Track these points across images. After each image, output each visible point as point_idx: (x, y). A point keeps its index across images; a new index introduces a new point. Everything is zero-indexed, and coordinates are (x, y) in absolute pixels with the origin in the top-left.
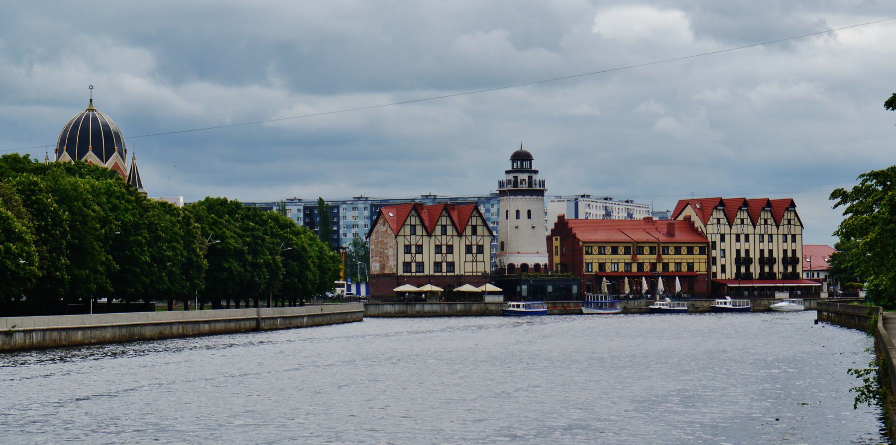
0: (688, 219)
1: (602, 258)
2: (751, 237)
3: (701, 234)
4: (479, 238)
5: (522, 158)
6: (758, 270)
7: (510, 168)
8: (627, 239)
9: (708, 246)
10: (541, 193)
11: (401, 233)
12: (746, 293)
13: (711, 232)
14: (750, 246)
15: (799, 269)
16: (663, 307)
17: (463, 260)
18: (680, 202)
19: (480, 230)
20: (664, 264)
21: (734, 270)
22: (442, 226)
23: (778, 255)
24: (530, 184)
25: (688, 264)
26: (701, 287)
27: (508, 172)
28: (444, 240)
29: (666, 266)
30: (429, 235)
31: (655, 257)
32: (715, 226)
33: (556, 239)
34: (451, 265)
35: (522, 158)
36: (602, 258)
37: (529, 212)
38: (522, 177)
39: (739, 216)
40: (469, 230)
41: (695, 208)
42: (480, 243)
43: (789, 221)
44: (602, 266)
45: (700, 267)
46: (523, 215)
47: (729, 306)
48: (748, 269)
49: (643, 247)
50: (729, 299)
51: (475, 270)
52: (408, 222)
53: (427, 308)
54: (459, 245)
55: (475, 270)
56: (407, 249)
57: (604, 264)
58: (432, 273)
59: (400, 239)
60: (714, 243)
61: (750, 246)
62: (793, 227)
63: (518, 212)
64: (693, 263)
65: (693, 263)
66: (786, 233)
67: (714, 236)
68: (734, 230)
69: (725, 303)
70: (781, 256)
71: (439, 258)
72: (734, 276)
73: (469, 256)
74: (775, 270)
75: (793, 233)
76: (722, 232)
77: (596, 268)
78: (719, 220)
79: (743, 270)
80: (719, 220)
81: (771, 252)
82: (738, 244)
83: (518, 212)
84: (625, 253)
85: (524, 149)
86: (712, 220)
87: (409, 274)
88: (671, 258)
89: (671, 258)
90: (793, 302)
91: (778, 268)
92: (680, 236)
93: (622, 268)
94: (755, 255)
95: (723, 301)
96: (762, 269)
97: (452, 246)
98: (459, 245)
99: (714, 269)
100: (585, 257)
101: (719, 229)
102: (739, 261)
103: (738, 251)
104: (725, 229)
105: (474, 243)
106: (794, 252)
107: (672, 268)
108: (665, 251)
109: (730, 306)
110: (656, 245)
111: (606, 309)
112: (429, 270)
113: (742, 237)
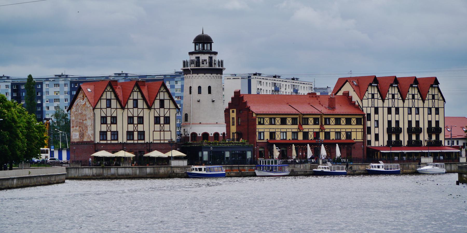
0: (346, 94)
1: (272, 128)
2: (401, 110)
3: (358, 107)
4: (166, 110)
5: (203, 41)
6: (407, 139)
7: (193, 50)
8: (294, 111)
9: (364, 118)
10: (219, 71)
11: (98, 106)
12: (396, 158)
13: (367, 105)
14: (400, 117)
15: (442, 138)
16: (325, 170)
17: (152, 129)
18: (340, 80)
19: (167, 103)
20: (325, 133)
22: (134, 100)
23: (424, 125)
24: (211, 64)
25: (347, 133)
26: (358, 153)
27: (191, 53)
28: (136, 112)
29: (327, 135)
30: (123, 108)
31: (318, 127)
32: (370, 100)
33: (233, 112)
34: (142, 134)
35: (203, 41)
36: (272, 128)
37: (210, 88)
38: (204, 57)
39: (390, 92)
40: (157, 104)
41: (352, 85)
42: (167, 115)
43: (433, 96)
44: (272, 135)
45: (357, 136)
46: (205, 90)
47: (381, 169)
48: (398, 137)
49: (308, 118)
50: (382, 164)
51: (162, 138)
52: (104, 97)
53: (121, 171)
54: (149, 116)
55: (162, 138)
56: (104, 120)
57: (275, 133)
58: (125, 141)
59: (97, 112)
60: (369, 115)
61: (400, 117)
62: (436, 101)
63: (200, 88)
64: (351, 132)
65: (351, 132)
66: (431, 106)
67: (369, 109)
68: (386, 104)
69: (379, 167)
70: (426, 126)
71: (131, 128)
72: (386, 144)
73: (157, 126)
74: (421, 138)
75: (436, 106)
76: (376, 106)
77: (267, 137)
78: (373, 95)
79: (394, 138)
80: (373, 95)
81: (417, 122)
82: (390, 116)
83: (200, 88)
84: (292, 124)
85: (204, 33)
86: (368, 95)
87: (105, 142)
88: (332, 128)
89: (332, 128)
90: (437, 166)
91: (424, 137)
92: (340, 109)
93: (289, 137)
94: (404, 126)
95: (377, 165)
96: (410, 137)
97: (142, 118)
98: (149, 116)
99: (369, 137)
100: (258, 127)
102: (390, 131)
103: (390, 122)
105: (162, 114)
106: (437, 122)
108: (327, 122)
109: (383, 170)
110: (319, 117)
111: (276, 172)
112: (122, 138)
113: (393, 110)
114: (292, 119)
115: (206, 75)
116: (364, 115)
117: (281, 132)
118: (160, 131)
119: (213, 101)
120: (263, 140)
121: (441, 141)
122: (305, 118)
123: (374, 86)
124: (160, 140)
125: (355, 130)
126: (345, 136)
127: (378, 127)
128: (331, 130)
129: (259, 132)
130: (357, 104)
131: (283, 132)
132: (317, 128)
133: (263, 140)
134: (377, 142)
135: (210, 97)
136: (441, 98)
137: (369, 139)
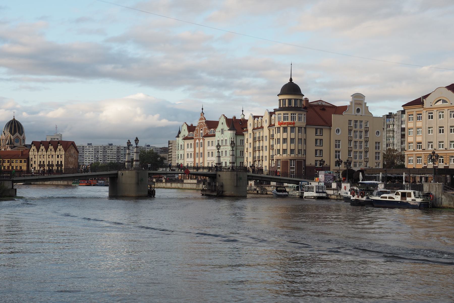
43: (60, 149)
78: (34, 150)
80: (34, 150)
86: (31, 150)
101: (34, 153)
103: (40, 162)
104: (36, 153)
106: (61, 162)
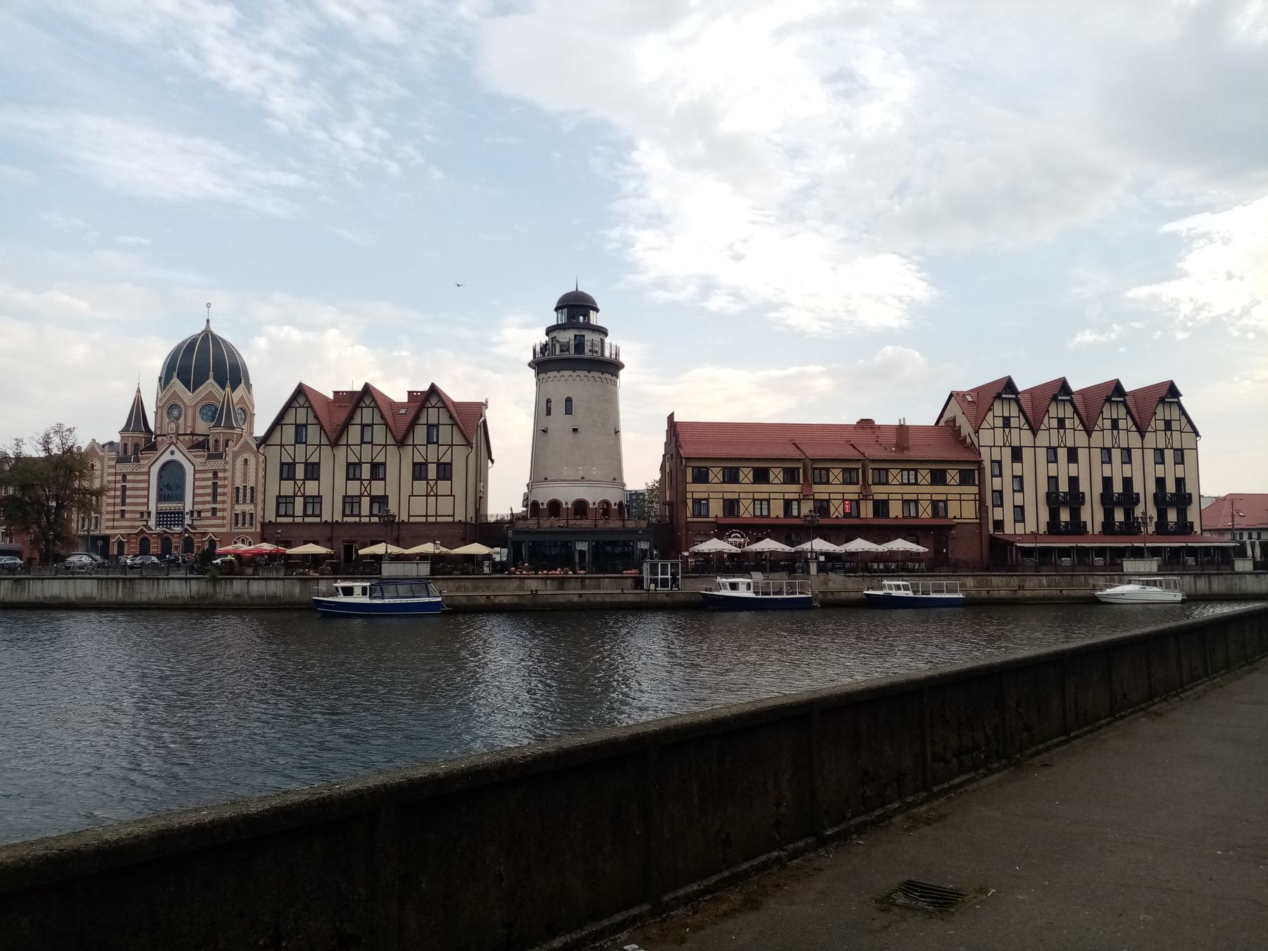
6: (1100, 517)
9: (981, 469)
13: (991, 443)
15: (1192, 515)
17: (406, 491)
19: (445, 433)
21: (1045, 516)
23: (1144, 488)
25: (935, 504)
32: (999, 432)
34: (382, 500)
37: (569, 401)
42: (446, 459)
44: (731, 506)
45: (962, 509)
46: (559, 407)
48: (1075, 514)
51: (431, 512)
55: (431, 512)
57: (738, 500)
58: (338, 517)
62: (1176, 435)
66: (1161, 445)
67: (996, 451)
68: (1043, 438)
73: (420, 486)
76: (1015, 443)
78: (1007, 422)
80: (1007, 422)
94: (1091, 488)
96: (1109, 514)
98: (399, 465)
100: (690, 487)
102: (1054, 500)
103: (1053, 480)
107: (895, 510)
114: (785, 470)
115: (562, 373)
116: (980, 463)
117: (754, 500)
118: (427, 495)
119: (575, 430)
120: (707, 516)
121: (1192, 523)
122: (821, 469)
123: (1010, 399)
124: (426, 516)
125: (958, 497)
126: (929, 510)
127: (1022, 490)
128: (891, 497)
129: (694, 500)
130: (968, 440)
131: (761, 500)
132: (853, 490)
133: (707, 516)
134: (1020, 526)
135: (569, 422)
136: (1188, 428)
137: (998, 517)
